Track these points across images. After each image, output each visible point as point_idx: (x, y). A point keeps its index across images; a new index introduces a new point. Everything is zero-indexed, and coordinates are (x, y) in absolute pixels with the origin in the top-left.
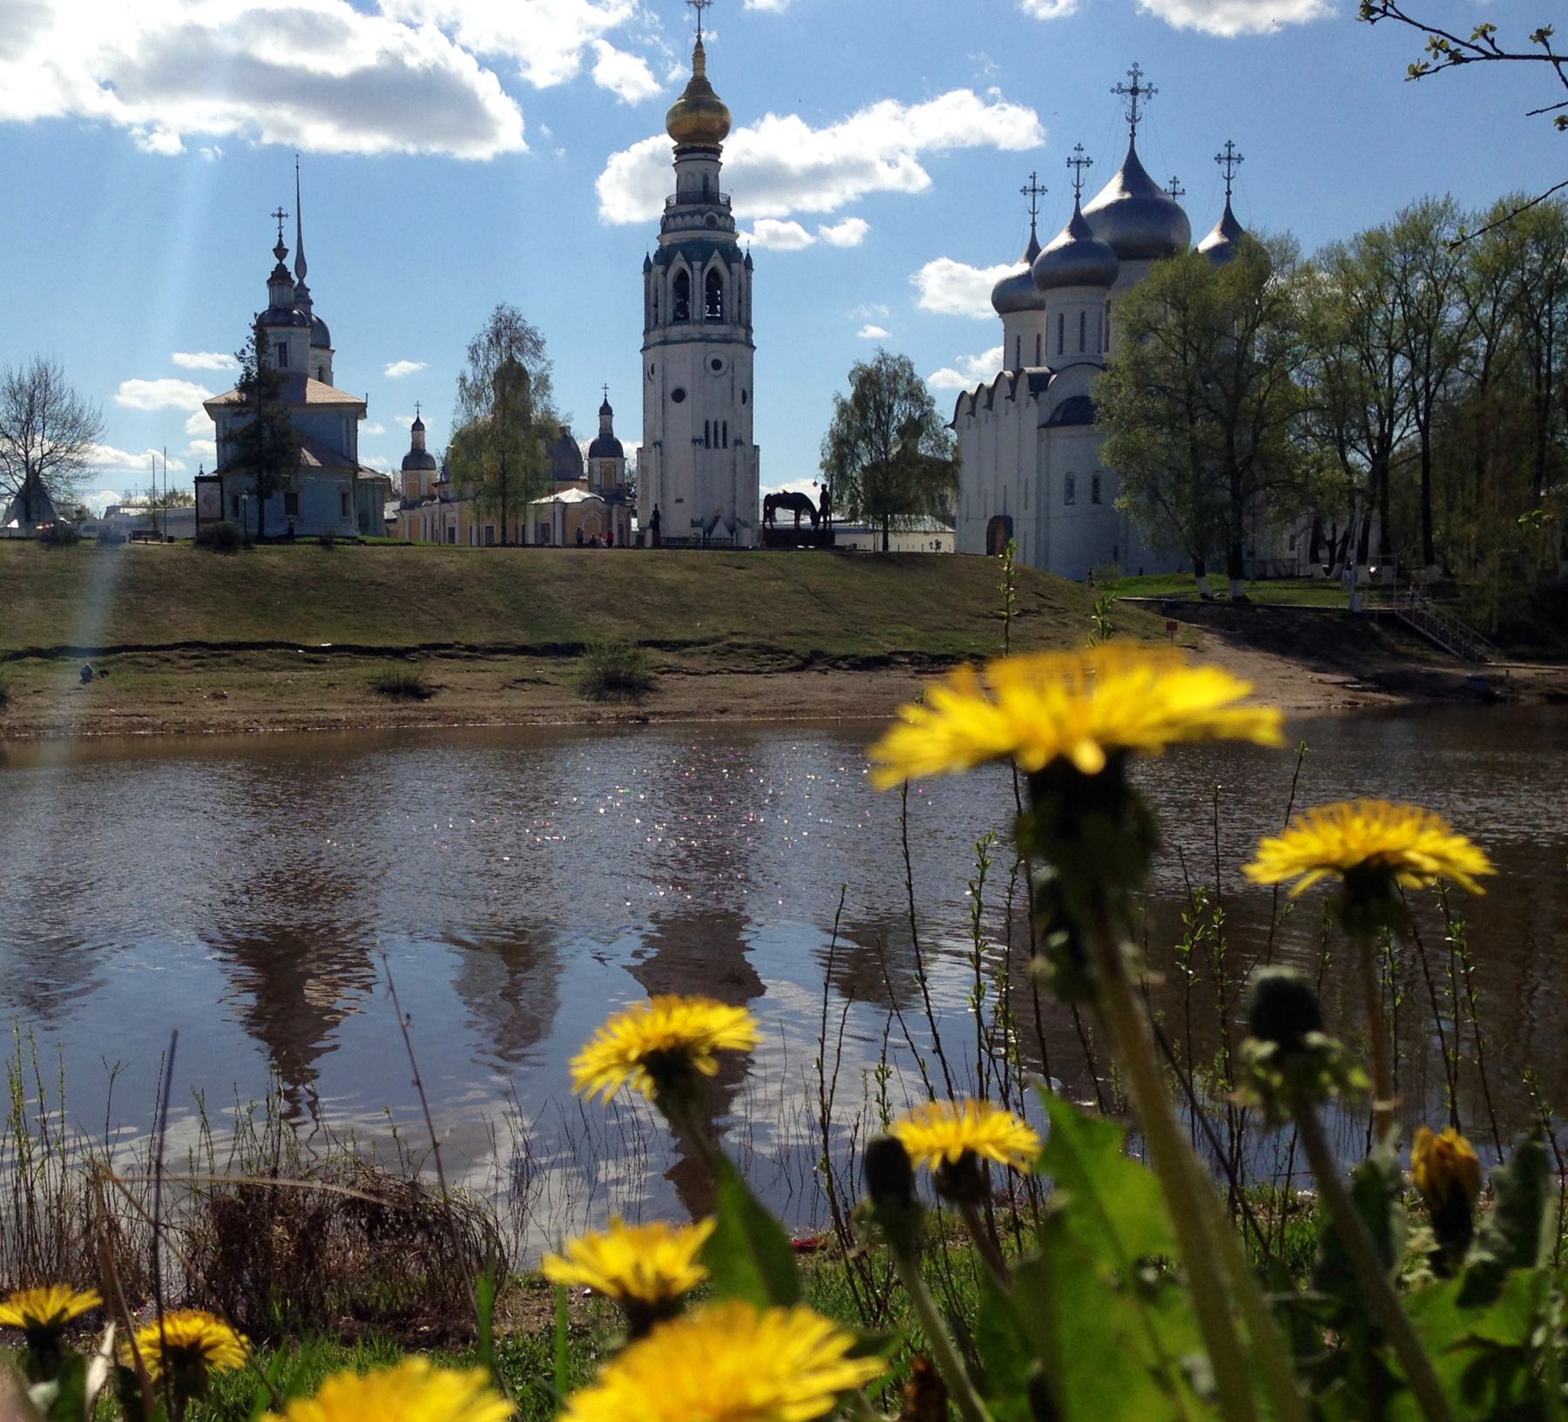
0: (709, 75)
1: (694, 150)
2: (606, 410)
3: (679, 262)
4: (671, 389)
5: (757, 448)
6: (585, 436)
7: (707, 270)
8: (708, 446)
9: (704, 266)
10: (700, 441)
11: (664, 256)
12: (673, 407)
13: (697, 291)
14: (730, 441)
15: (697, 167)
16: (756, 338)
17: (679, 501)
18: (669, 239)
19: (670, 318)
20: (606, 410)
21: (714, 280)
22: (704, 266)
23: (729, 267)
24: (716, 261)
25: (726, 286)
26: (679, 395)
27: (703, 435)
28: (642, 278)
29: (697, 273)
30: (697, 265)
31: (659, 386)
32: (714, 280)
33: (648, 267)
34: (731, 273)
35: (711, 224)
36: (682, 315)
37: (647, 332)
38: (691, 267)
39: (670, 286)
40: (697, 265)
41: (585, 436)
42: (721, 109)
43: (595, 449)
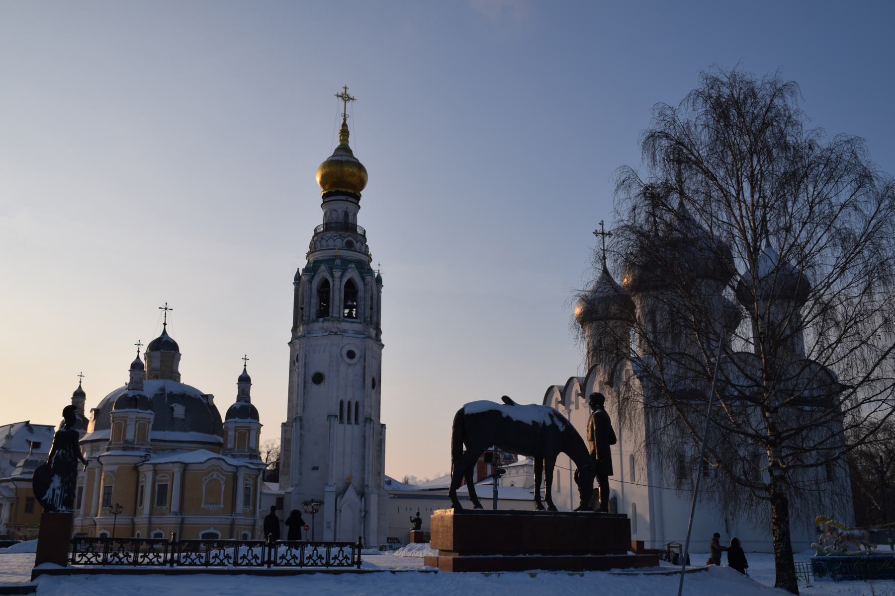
0: (351, 145)
1: (338, 193)
2: (244, 381)
3: (323, 272)
4: (311, 373)
5: (383, 426)
6: (224, 402)
7: (345, 280)
8: (341, 421)
9: (342, 276)
10: (336, 416)
11: (312, 269)
12: (314, 388)
13: (337, 294)
14: (361, 419)
15: (341, 206)
16: (384, 338)
17: (315, 468)
18: (318, 255)
19: (313, 316)
20: (244, 381)
21: (350, 287)
22: (342, 276)
23: (363, 279)
24: (352, 273)
25: (361, 294)
26: (318, 378)
27: (338, 414)
28: (293, 287)
29: (337, 280)
30: (337, 274)
31: (302, 370)
32: (350, 287)
33: (298, 278)
34: (365, 285)
35: (350, 246)
36: (324, 313)
37: (294, 330)
38: (332, 276)
39: (315, 292)
40: (337, 274)
41: (224, 402)
42: (361, 167)
43: (231, 412)
